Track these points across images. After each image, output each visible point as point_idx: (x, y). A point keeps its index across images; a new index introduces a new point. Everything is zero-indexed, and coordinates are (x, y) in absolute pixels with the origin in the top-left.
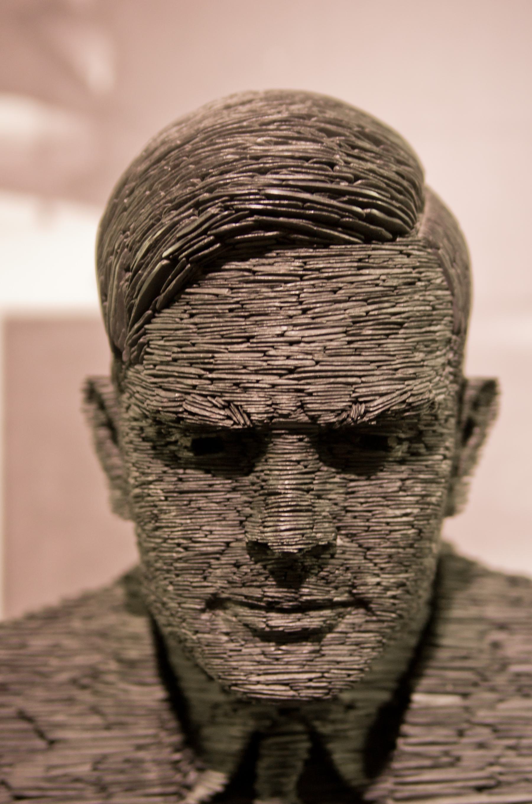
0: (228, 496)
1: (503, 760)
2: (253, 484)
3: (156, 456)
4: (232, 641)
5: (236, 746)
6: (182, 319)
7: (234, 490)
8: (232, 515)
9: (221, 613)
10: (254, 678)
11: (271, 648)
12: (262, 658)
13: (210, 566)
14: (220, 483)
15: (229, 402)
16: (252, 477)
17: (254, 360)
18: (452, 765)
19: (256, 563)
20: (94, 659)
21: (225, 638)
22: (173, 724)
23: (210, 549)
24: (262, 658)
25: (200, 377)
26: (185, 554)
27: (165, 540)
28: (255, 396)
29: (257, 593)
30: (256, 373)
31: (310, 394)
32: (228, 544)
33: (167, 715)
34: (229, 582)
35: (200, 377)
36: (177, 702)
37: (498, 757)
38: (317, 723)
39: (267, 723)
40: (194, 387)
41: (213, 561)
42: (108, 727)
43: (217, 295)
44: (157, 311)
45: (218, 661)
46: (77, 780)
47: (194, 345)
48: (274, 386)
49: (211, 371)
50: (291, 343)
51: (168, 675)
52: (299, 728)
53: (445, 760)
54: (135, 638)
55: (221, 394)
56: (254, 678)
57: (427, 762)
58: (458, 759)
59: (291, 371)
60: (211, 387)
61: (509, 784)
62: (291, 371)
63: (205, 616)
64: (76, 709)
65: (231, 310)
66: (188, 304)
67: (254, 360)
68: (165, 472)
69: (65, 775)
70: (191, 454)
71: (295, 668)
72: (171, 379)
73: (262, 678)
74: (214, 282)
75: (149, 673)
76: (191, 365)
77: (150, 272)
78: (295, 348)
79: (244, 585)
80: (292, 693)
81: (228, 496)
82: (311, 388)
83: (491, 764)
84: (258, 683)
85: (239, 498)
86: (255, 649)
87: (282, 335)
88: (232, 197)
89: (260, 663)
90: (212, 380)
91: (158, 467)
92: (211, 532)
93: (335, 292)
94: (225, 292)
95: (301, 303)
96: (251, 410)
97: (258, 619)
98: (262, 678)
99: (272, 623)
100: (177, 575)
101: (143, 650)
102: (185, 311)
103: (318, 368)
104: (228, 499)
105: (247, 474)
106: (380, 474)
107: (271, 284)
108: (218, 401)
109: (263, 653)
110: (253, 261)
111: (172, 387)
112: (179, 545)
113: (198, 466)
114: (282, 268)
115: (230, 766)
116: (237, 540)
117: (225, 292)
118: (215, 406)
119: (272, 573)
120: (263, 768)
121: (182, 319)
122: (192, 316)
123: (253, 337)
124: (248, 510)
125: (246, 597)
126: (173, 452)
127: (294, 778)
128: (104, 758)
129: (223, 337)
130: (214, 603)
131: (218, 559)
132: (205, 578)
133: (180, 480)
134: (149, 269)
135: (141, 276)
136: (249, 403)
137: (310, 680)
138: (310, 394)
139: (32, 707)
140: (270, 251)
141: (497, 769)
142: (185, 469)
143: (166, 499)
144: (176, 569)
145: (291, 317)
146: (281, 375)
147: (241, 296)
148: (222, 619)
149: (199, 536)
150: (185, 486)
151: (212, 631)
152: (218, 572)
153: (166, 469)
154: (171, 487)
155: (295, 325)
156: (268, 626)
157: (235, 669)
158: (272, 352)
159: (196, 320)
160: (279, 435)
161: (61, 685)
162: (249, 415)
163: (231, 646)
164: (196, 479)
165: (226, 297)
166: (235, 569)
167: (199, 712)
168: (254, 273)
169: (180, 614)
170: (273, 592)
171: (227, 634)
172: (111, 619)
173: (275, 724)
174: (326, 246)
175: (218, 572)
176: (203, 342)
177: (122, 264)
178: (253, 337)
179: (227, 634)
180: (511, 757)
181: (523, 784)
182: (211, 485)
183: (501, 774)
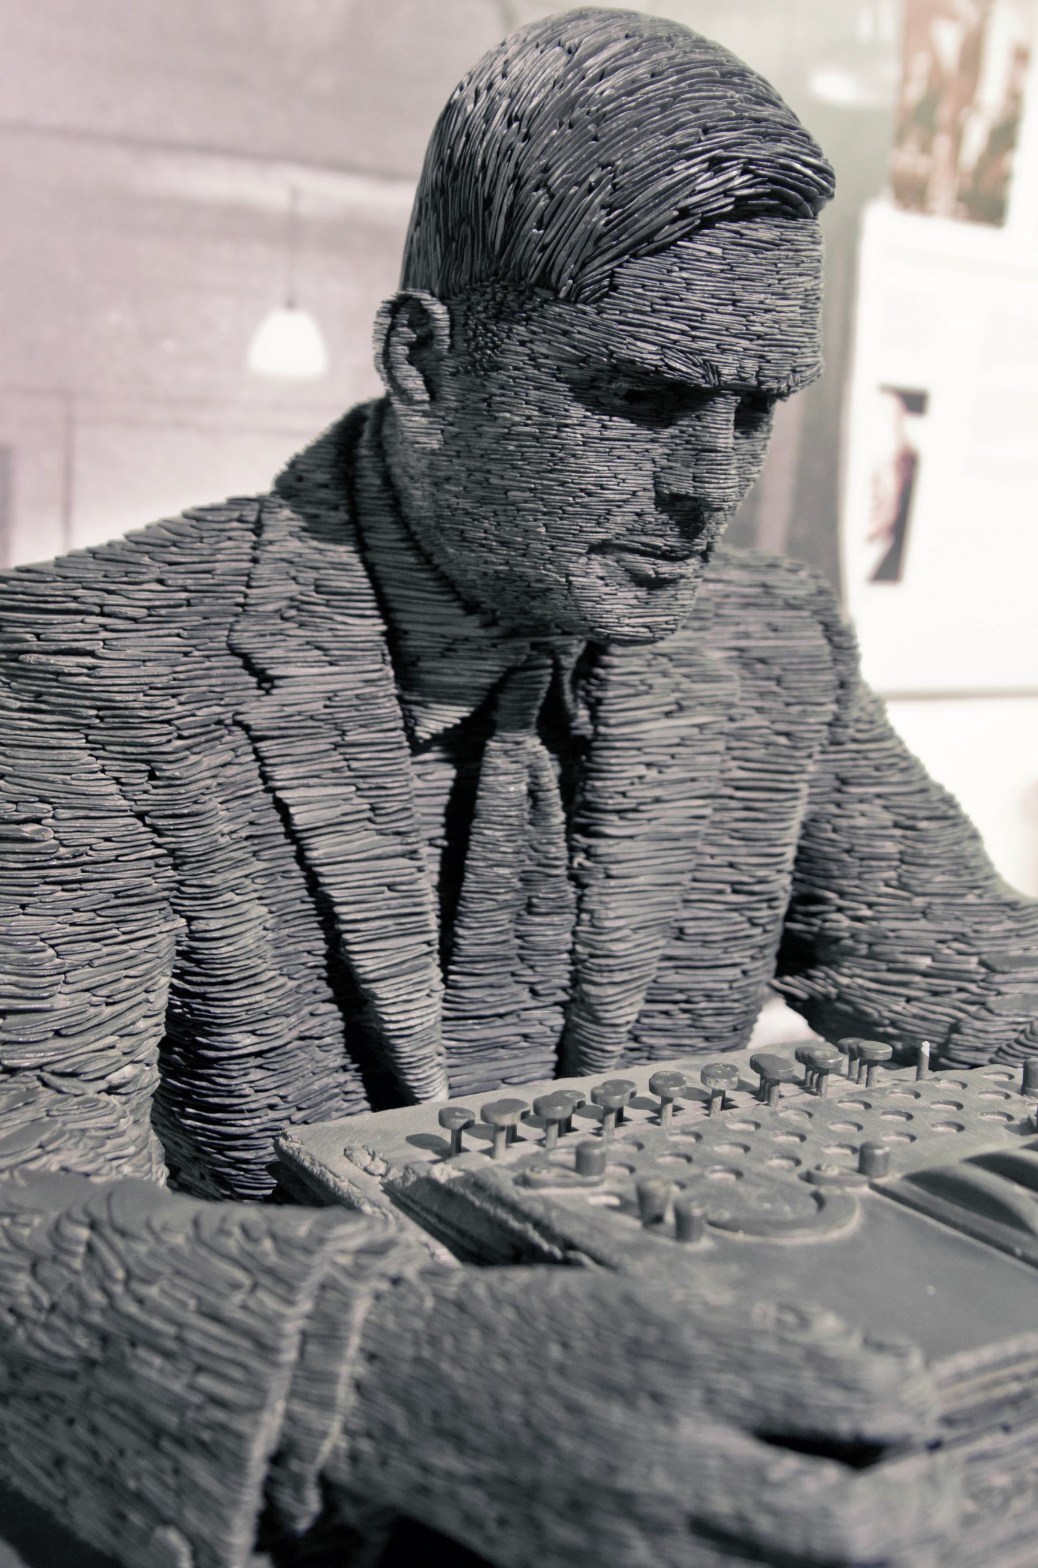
0: (648, 446)
1: (682, 687)
2: (673, 437)
3: (577, 399)
4: (606, 585)
5: (485, 680)
6: (669, 271)
7: (652, 441)
8: (649, 466)
9: (599, 558)
10: (627, 621)
11: (642, 593)
12: (634, 602)
13: (609, 512)
14: (645, 433)
15: (705, 361)
16: (672, 431)
17: (736, 324)
18: (647, 693)
19: (661, 513)
20: (293, 589)
21: (601, 582)
22: (389, 658)
23: (618, 497)
24: (634, 602)
25: (683, 333)
26: (587, 499)
27: (563, 484)
28: (730, 358)
29: (659, 542)
30: (735, 336)
31: (769, 362)
32: (634, 493)
33: (386, 649)
34: (628, 530)
35: (683, 333)
36: (393, 637)
37: (678, 684)
38: (562, 657)
39: (524, 657)
40: (675, 342)
41: (615, 509)
42: (331, 664)
43: (709, 253)
44: (635, 256)
45: (590, 604)
46: (312, 718)
47: (681, 300)
48: (745, 349)
49: (694, 328)
50: (767, 311)
51: (385, 609)
52: (549, 662)
53: (644, 688)
54: (342, 567)
55: (700, 352)
56: (627, 621)
57: (631, 691)
58: (651, 686)
59: (759, 337)
60: (694, 345)
61: (689, 707)
62: (759, 337)
63: (583, 560)
64: (293, 643)
65: (722, 271)
66: (676, 256)
67: (736, 324)
68: (585, 417)
69: (300, 713)
70: (623, 402)
71: (658, 611)
72: (649, 331)
73: (632, 621)
74: (707, 239)
75: (369, 605)
76: (672, 319)
77: (652, 220)
78: (768, 316)
79: (646, 534)
80: (650, 635)
81: (648, 446)
82: (771, 356)
83: (674, 691)
84: (628, 625)
85: (657, 450)
86: (630, 594)
87: (761, 302)
88: (751, 161)
89: (633, 607)
90: (694, 338)
91: (577, 411)
92: (624, 481)
93: (797, 265)
94: (718, 251)
95: (778, 273)
96: (725, 371)
97: (647, 567)
98: (632, 621)
99: (660, 570)
100: (561, 519)
101: (358, 580)
102: (674, 264)
103: (779, 337)
104: (647, 450)
105: (666, 427)
106: (757, 434)
107: (756, 250)
108: (698, 359)
109: (636, 598)
110: (744, 223)
111: (649, 338)
112: (582, 490)
113: (623, 415)
114: (765, 234)
115: (477, 700)
116: (645, 490)
117: (718, 251)
118: (695, 365)
119: (678, 524)
120: (506, 699)
121: (669, 271)
122: (681, 269)
123: (739, 301)
124: (664, 463)
125: (643, 544)
126: (597, 397)
127: (536, 712)
128: (335, 693)
129: (713, 297)
130: (601, 548)
131: (619, 507)
132: (599, 523)
133: (604, 427)
134: (652, 215)
135: (637, 221)
136: (726, 364)
137: (667, 623)
138: (769, 362)
139: (245, 640)
140: (757, 216)
141: (678, 695)
142: (611, 416)
143: (584, 444)
144: (564, 512)
145: (770, 285)
146: (751, 340)
147: (731, 258)
148: (597, 565)
149: (612, 483)
150: (607, 434)
151: (587, 575)
152: (619, 519)
153: (589, 414)
154: (596, 433)
155: (773, 294)
156: (656, 573)
157: (607, 612)
158: (752, 318)
159: (685, 275)
160: (724, 396)
161: (268, 615)
162: (719, 375)
163: (607, 590)
164: (621, 426)
165: (717, 257)
166: (635, 518)
167: (413, 644)
168: (742, 235)
169: (547, 556)
170: (672, 540)
171: (602, 578)
172: (294, 545)
173: (530, 658)
174: (794, 218)
175: (619, 519)
176: (694, 299)
177: (603, 200)
178: (739, 301)
179: (602, 578)
180: (686, 684)
181: (699, 708)
182: (633, 435)
183: (684, 699)
